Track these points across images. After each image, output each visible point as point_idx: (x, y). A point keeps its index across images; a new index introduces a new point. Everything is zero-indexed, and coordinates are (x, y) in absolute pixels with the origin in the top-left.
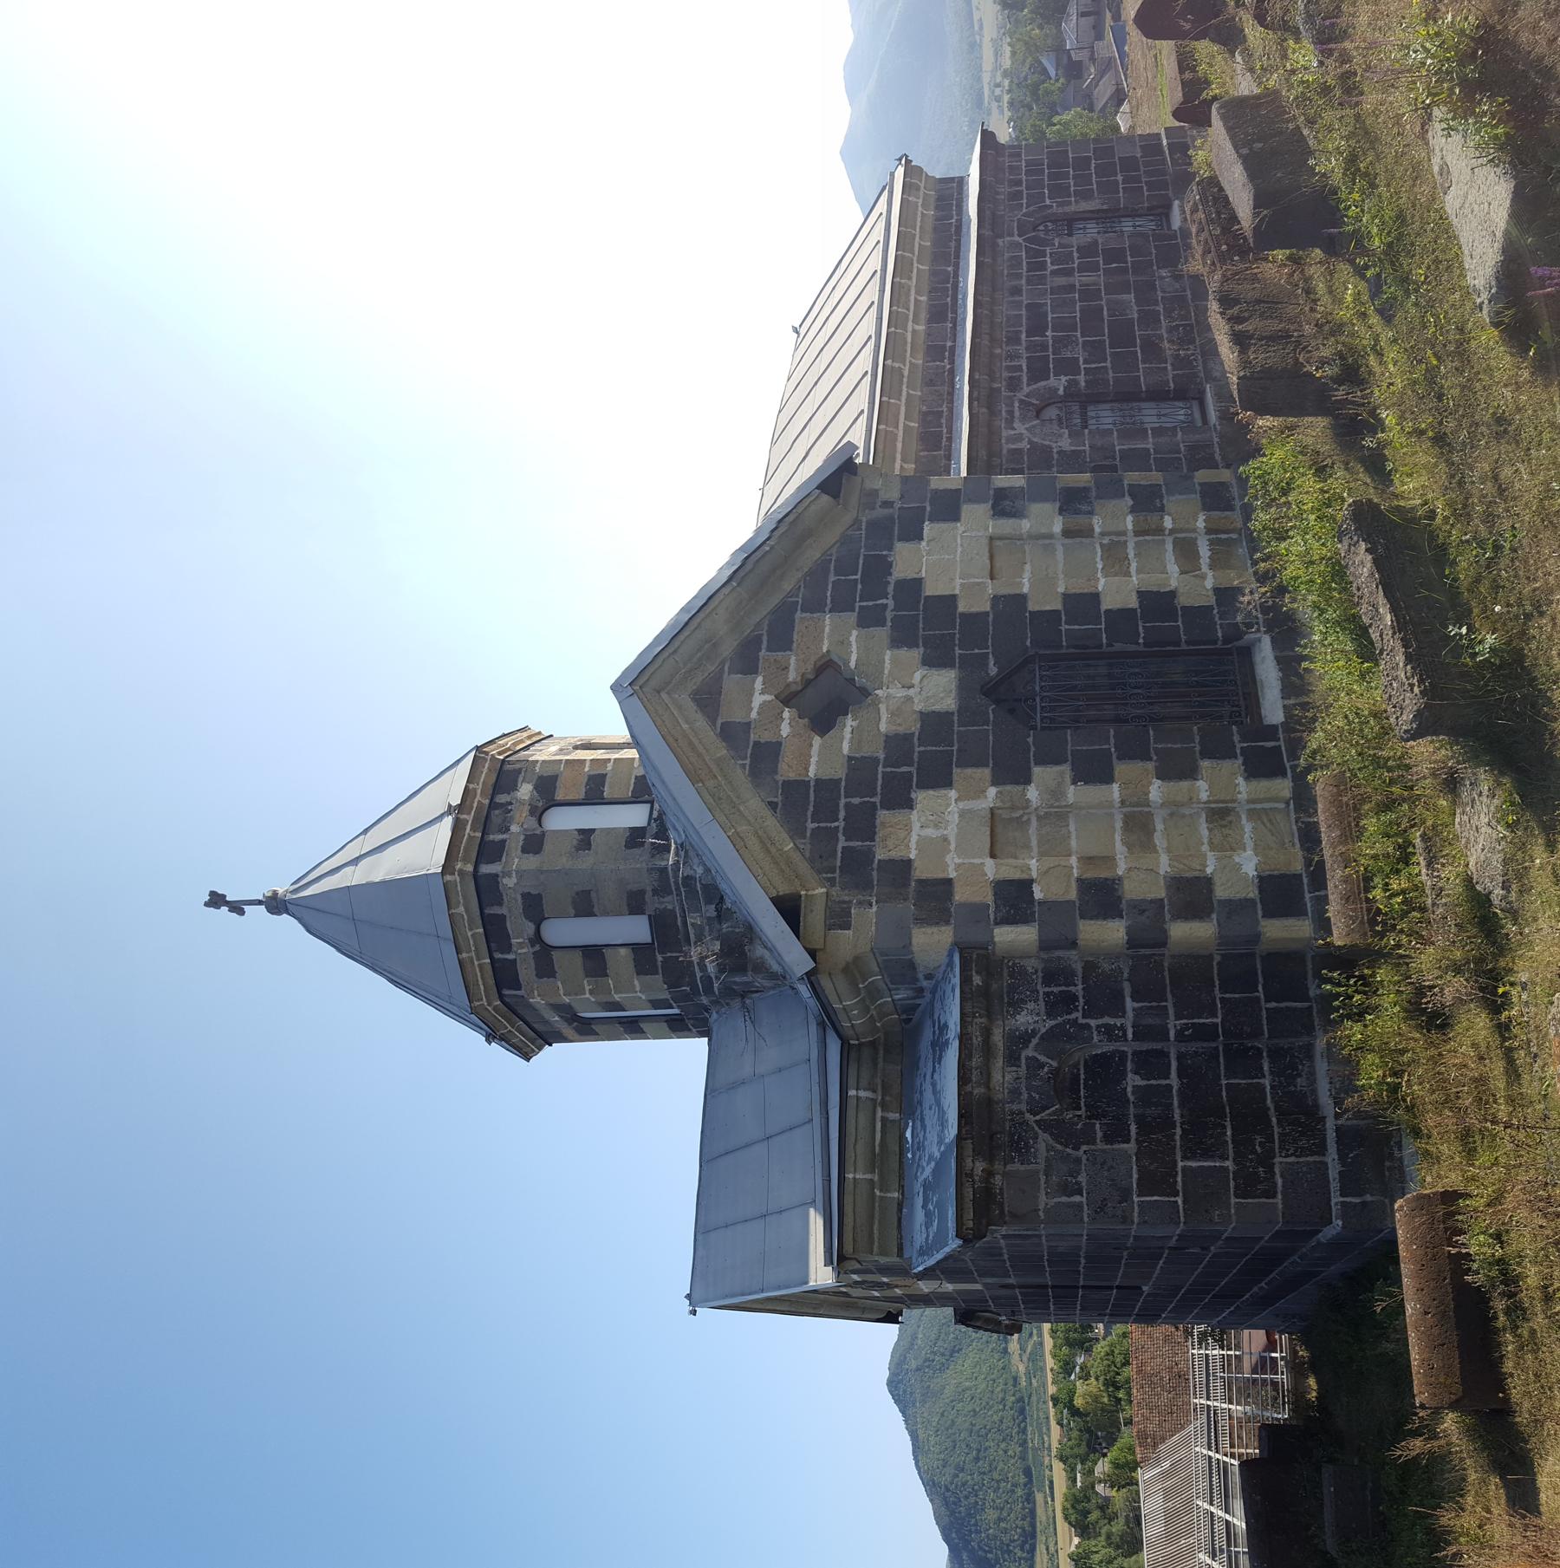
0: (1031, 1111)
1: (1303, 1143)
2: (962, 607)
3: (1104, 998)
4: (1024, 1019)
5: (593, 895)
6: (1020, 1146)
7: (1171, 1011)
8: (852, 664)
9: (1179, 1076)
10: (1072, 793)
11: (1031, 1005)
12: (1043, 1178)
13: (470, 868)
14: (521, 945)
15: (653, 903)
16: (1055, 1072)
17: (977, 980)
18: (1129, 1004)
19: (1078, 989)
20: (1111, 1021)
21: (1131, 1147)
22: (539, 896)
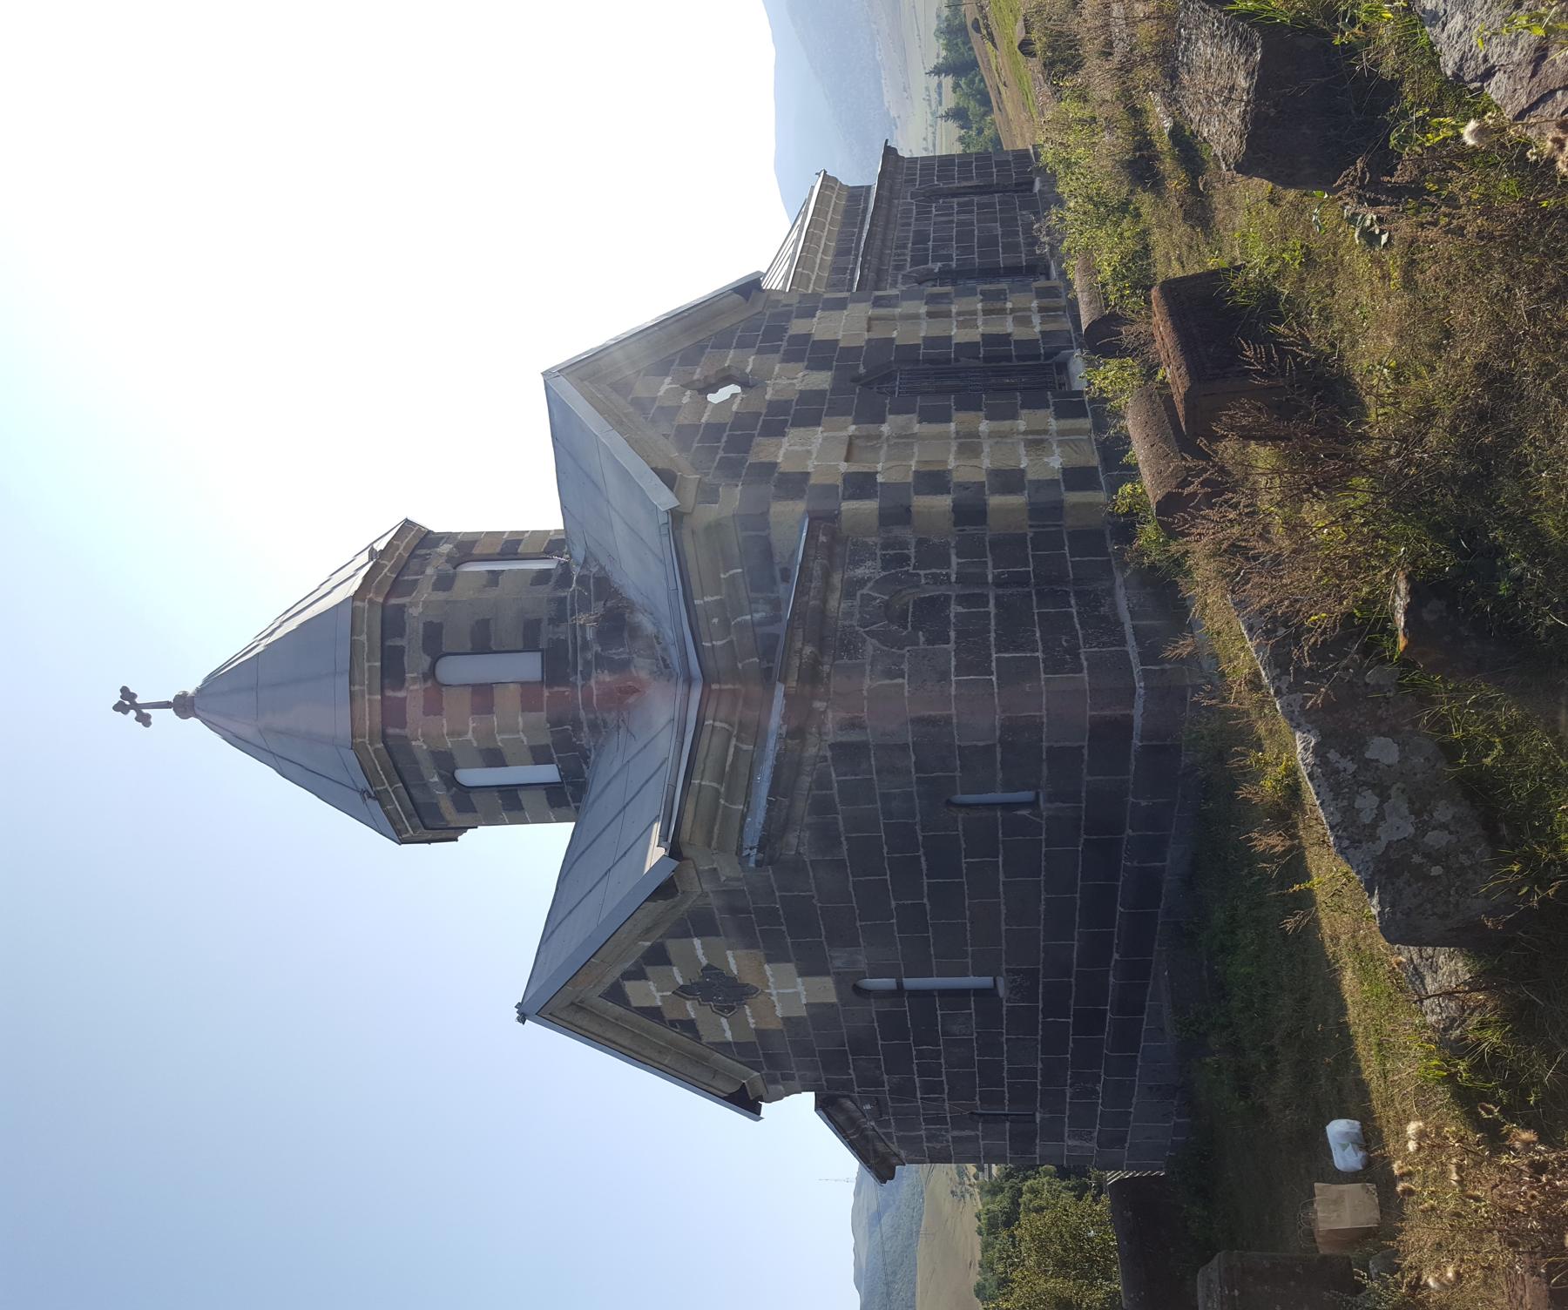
1: (1105, 639)
4: (860, 572)
7: (990, 564)
9: (997, 605)
10: (917, 428)
11: (869, 563)
12: (868, 668)
15: (546, 635)
16: (887, 605)
17: (822, 539)
18: (954, 560)
19: (912, 552)
21: (952, 646)
22: (440, 626)
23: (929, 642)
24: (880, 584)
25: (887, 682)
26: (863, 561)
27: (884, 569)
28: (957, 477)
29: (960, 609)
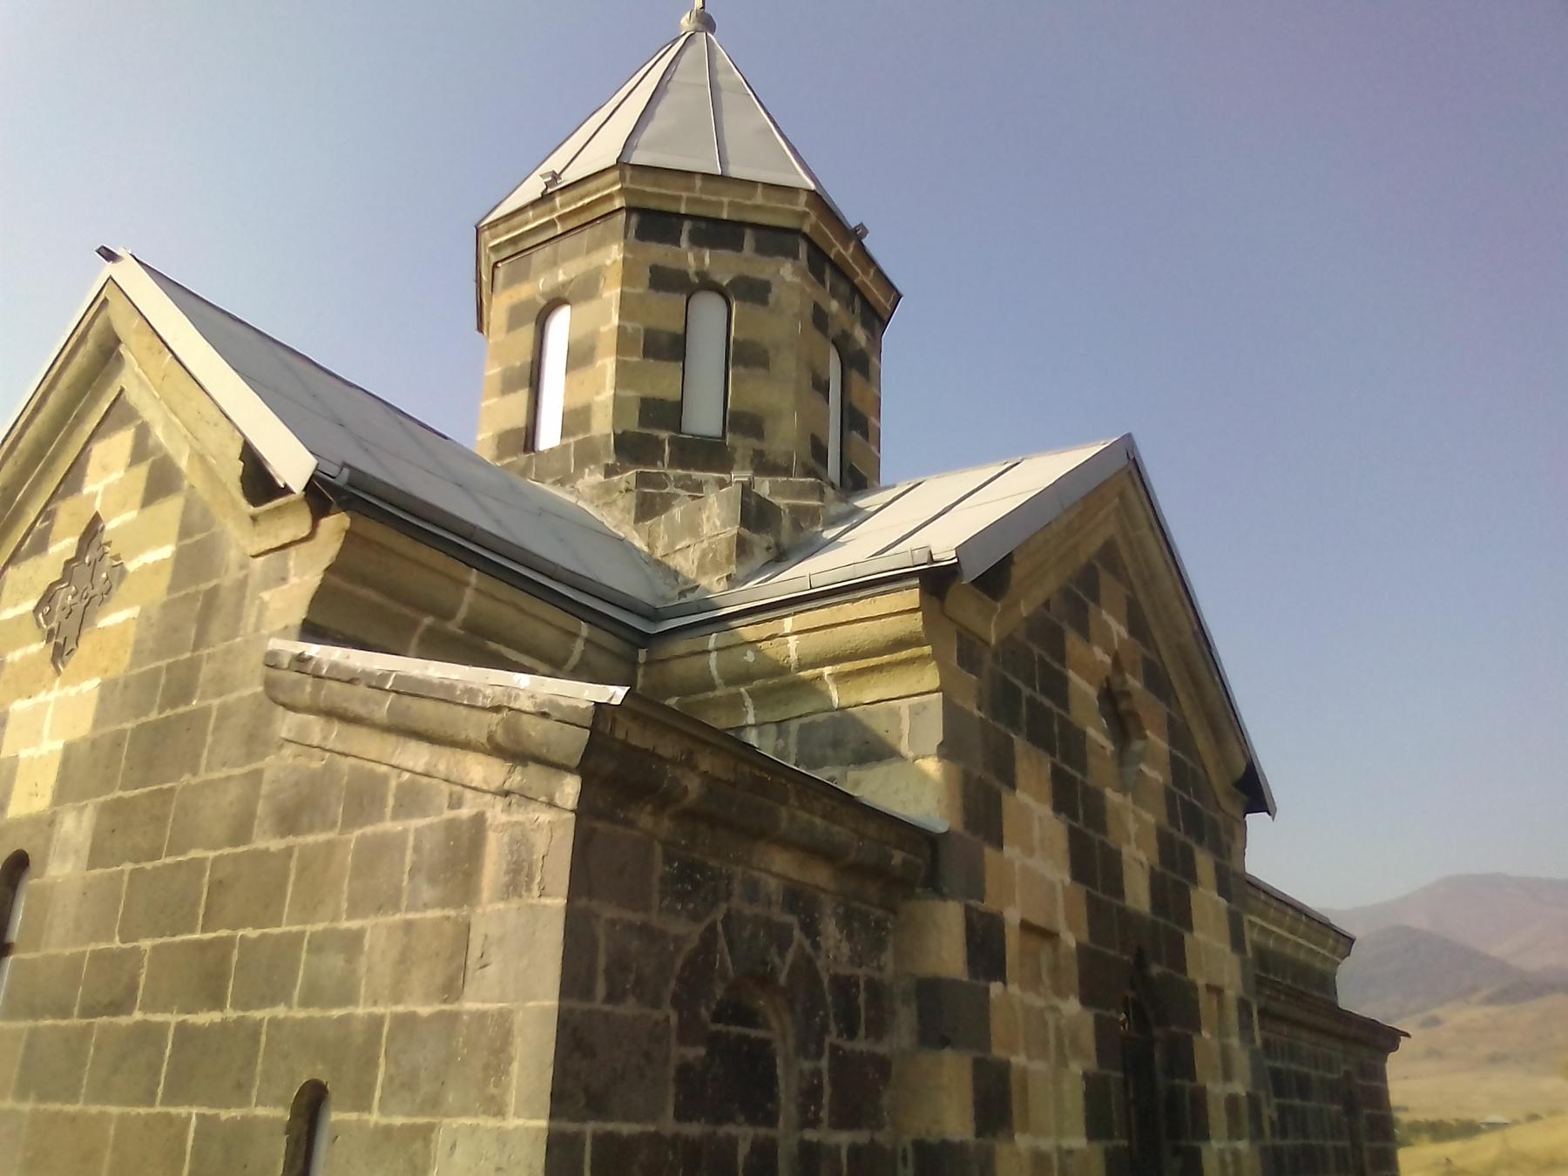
0: (728, 916)
2: (1187, 937)
3: (859, 1090)
4: (830, 929)
5: (761, 372)
6: (691, 882)
8: (1143, 767)
10: (1076, 1068)
11: (845, 948)
12: (636, 917)
13: (806, 229)
14: (700, 259)
15: (740, 444)
16: (765, 981)
18: (843, 1138)
20: (825, 1100)
21: (668, 1125)
22: (763, 301)
23: (684, 1070)
24: (806, 969)
25: (602, 961)
26: (850, 937)
27: (835, 979)
28: (1002, 1150)
29: (743, 1149)
